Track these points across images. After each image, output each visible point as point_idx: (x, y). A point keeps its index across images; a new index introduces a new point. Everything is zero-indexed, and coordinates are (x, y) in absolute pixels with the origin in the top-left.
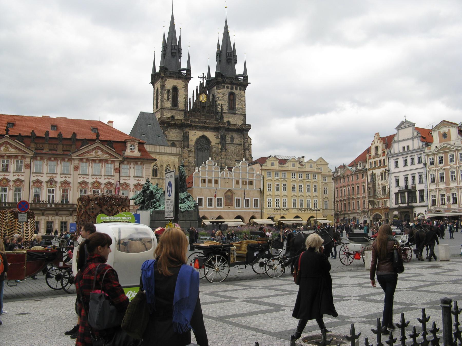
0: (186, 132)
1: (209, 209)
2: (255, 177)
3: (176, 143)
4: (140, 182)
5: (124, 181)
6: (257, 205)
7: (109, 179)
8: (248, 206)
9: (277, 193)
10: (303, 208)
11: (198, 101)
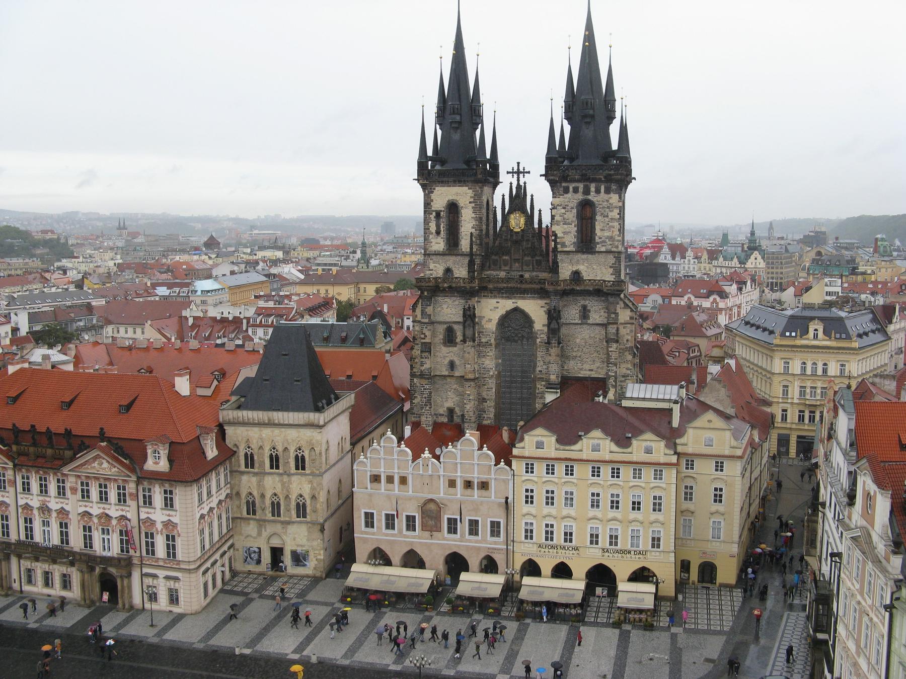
0: (469, 308)
1: (387, 535)
2: (493, 472)
3: (455, 327)
4: (171, 518)
5: (146, 515)
6: (499, 532)
7: (122, 510)
8: (477, 534)
10: (619, 547)
11: (504, 229)
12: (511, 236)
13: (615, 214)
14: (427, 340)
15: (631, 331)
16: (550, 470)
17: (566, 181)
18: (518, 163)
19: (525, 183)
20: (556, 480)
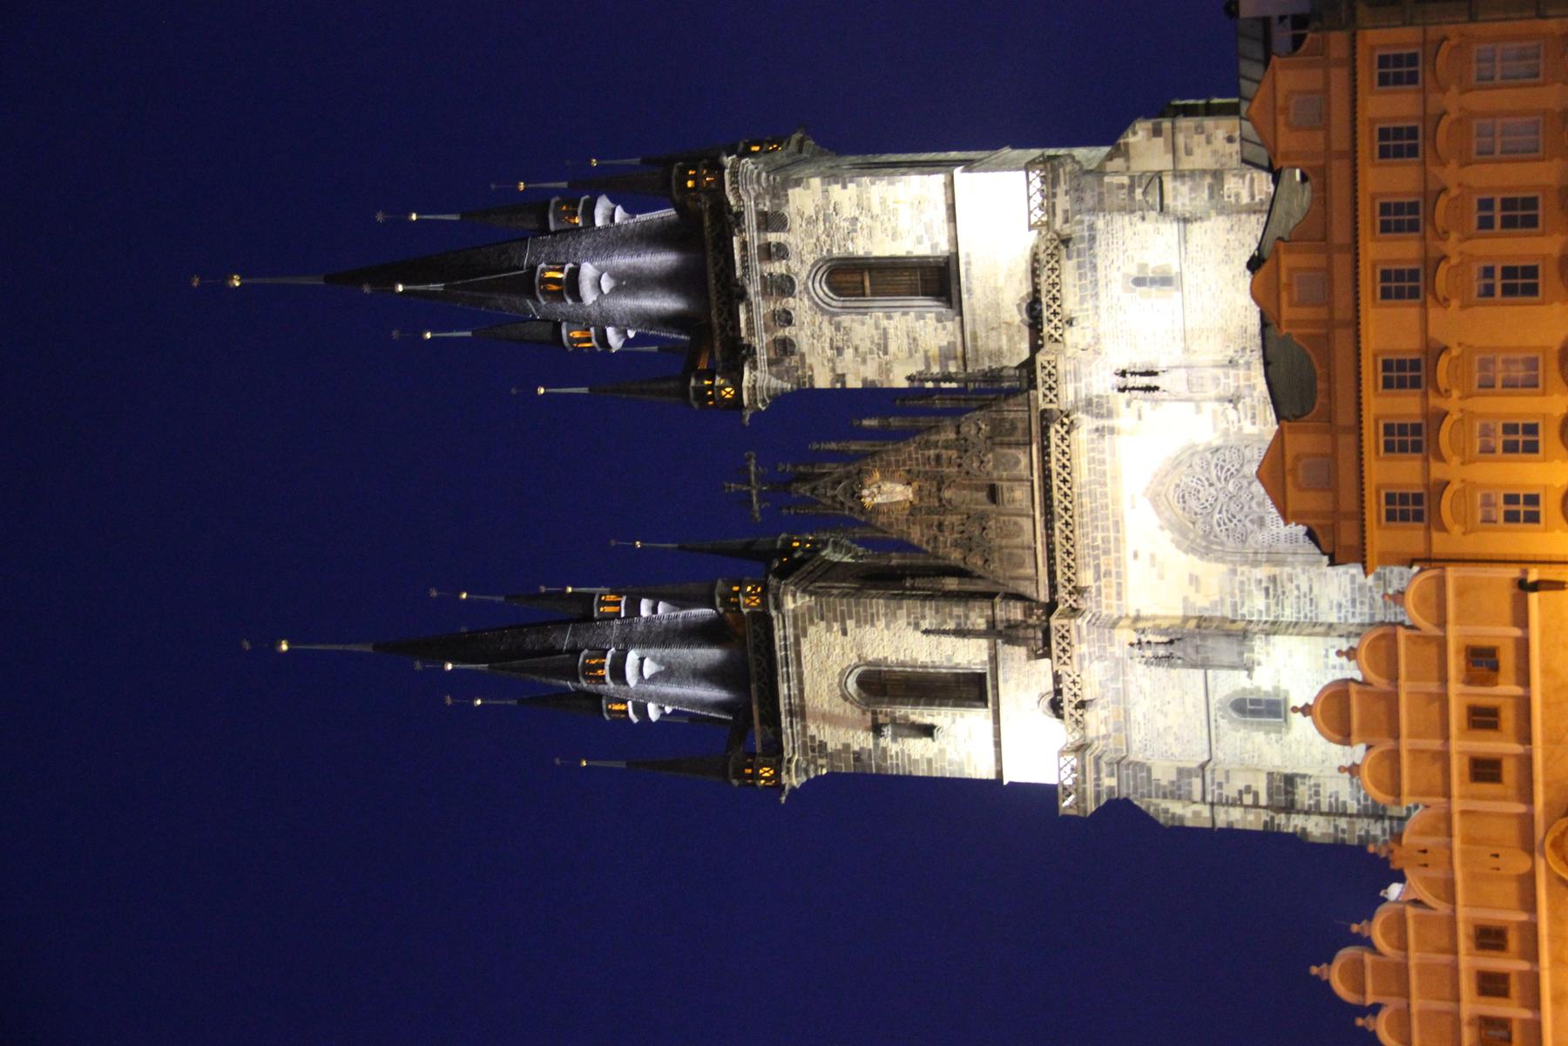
12: (930, 511)
14: (1261, 786)
15: (1200, 130)
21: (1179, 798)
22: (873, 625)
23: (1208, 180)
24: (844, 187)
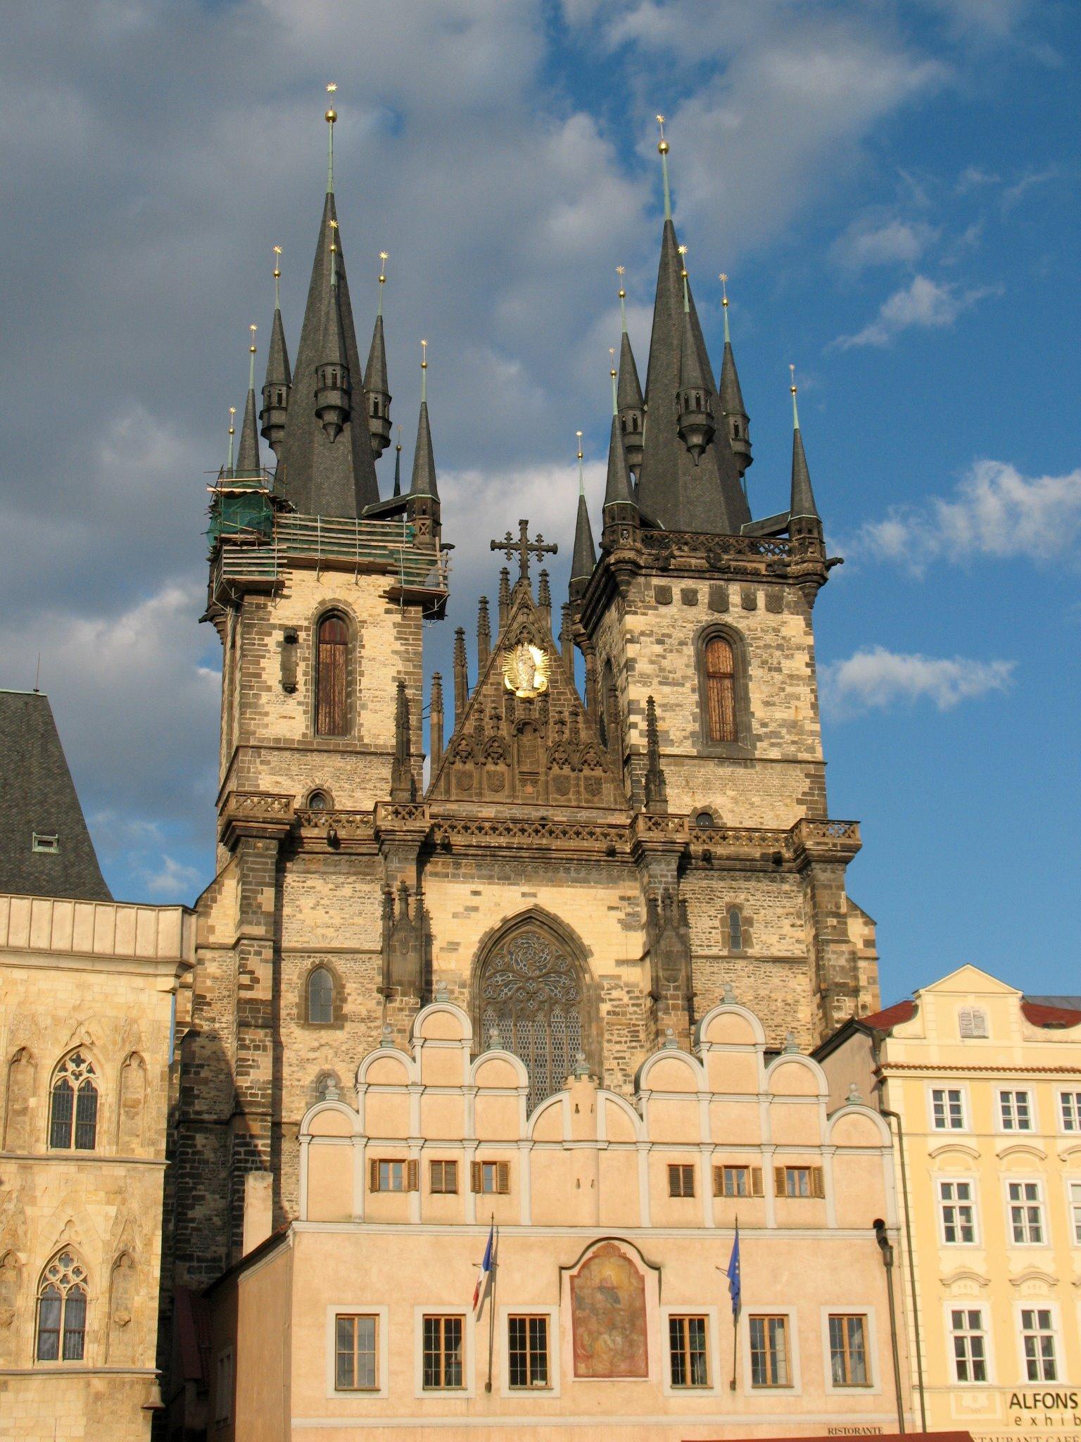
0: (404, 890)
9: (1023, 1256)
11: (487, 690)
12: (510, 709)
13: (799, 664)
15: (872, 981)
16: (1016, 1110)
17: (665, 570)
18: (524, 524)
19: (544, 574)
20: (1039, 1144)
21: (243, 912)
22: (397, 639)
23: (852, 983)
24: (808, 665)
